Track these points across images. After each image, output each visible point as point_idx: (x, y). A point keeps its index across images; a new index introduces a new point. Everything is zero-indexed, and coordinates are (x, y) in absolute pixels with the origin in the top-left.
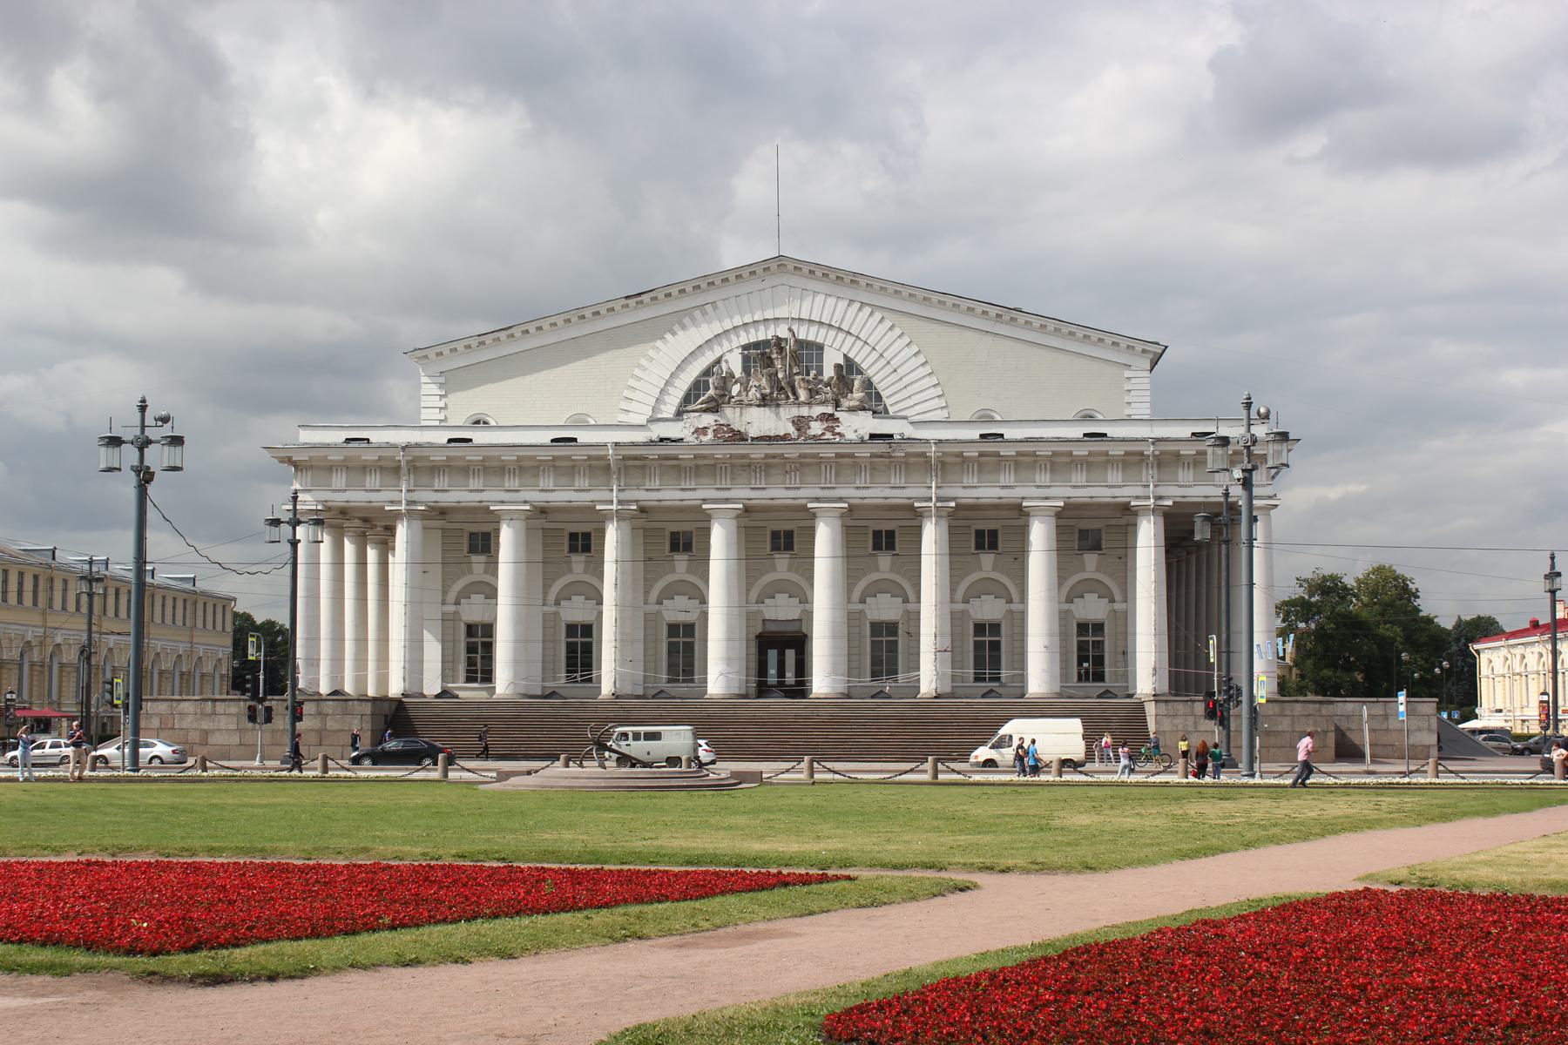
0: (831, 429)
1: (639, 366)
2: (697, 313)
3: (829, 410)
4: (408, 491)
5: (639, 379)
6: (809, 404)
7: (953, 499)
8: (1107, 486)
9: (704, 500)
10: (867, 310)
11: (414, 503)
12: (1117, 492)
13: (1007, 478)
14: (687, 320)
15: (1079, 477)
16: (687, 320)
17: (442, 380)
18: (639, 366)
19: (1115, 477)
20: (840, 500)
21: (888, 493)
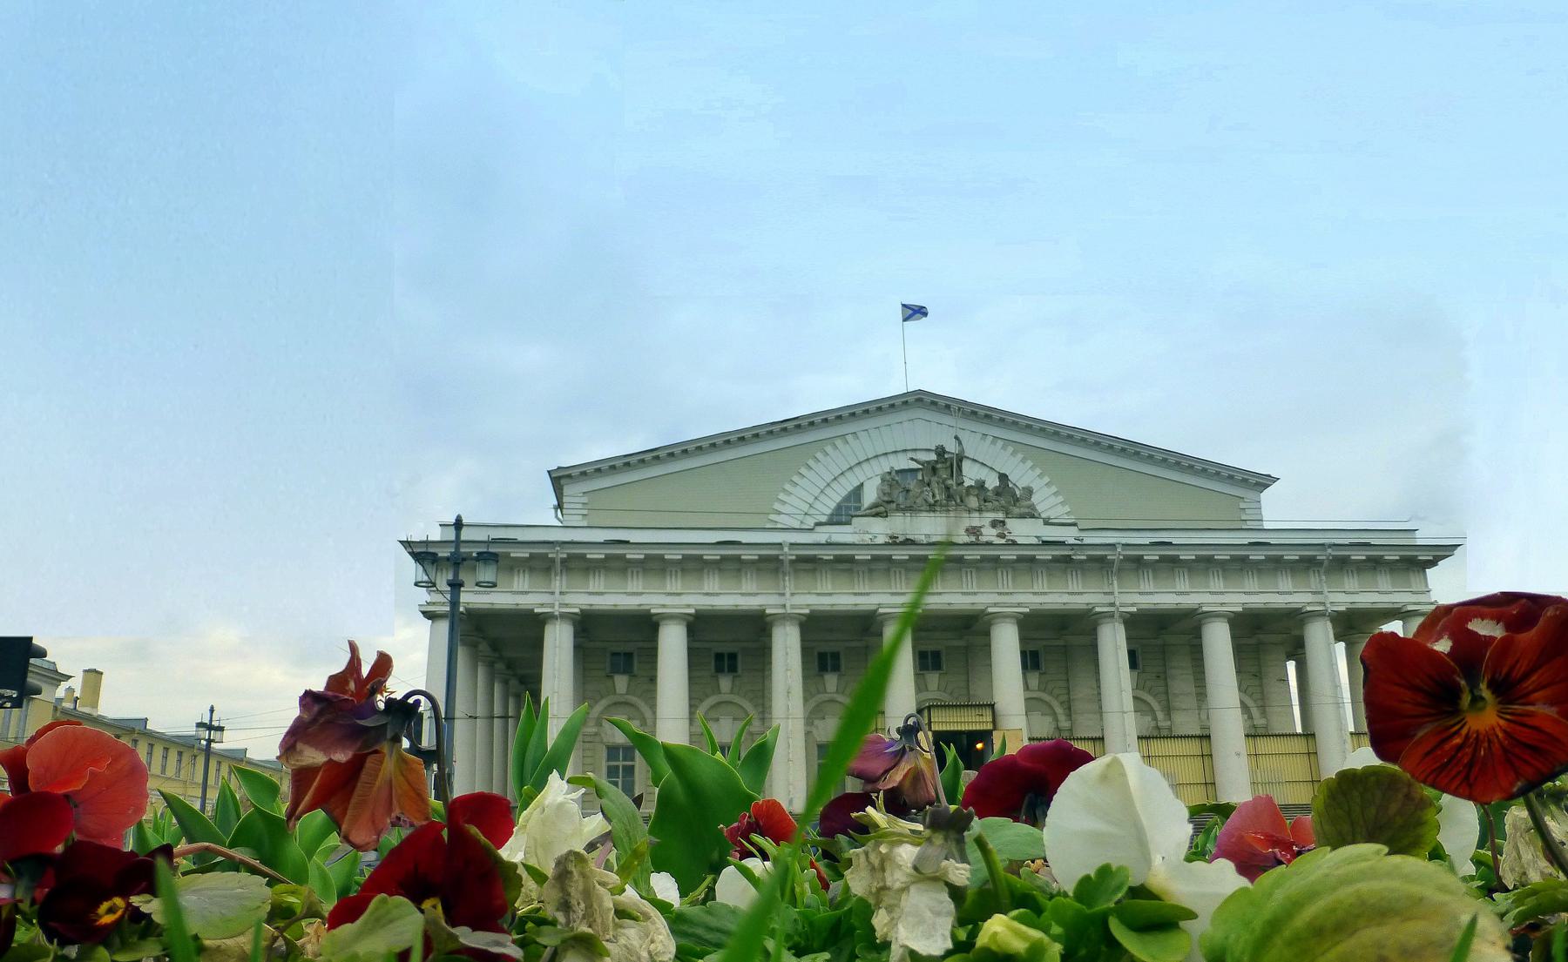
0: (1002, 536)
1: (784, 490)
2: (839, 442)
3: (1000, 516)
4: (561, 593)
5: (784, 503)
6: (980, 510)
7: (1133, 605)
8: (1278, 593)
9: (879, 604)
10: (1000, 443)
11: (567, 605)
12: (1289, 599)
13: (1183, 584)
14: (829, 449)
15: (1252, 583)
16: (829, 449)
17: (585, 500)
18: (784, 490)
19: (1285, 583)
20: (1019, 605)
21: (1066, 599)
